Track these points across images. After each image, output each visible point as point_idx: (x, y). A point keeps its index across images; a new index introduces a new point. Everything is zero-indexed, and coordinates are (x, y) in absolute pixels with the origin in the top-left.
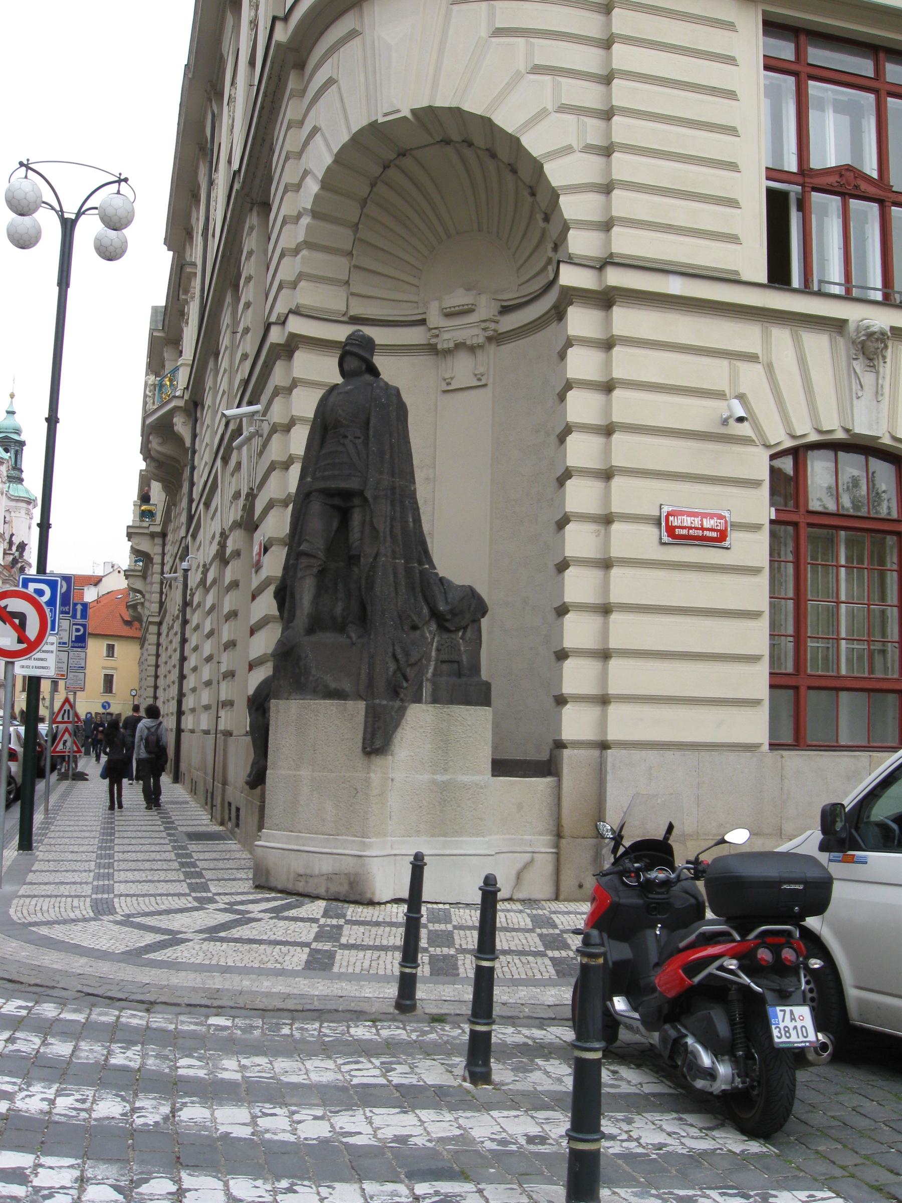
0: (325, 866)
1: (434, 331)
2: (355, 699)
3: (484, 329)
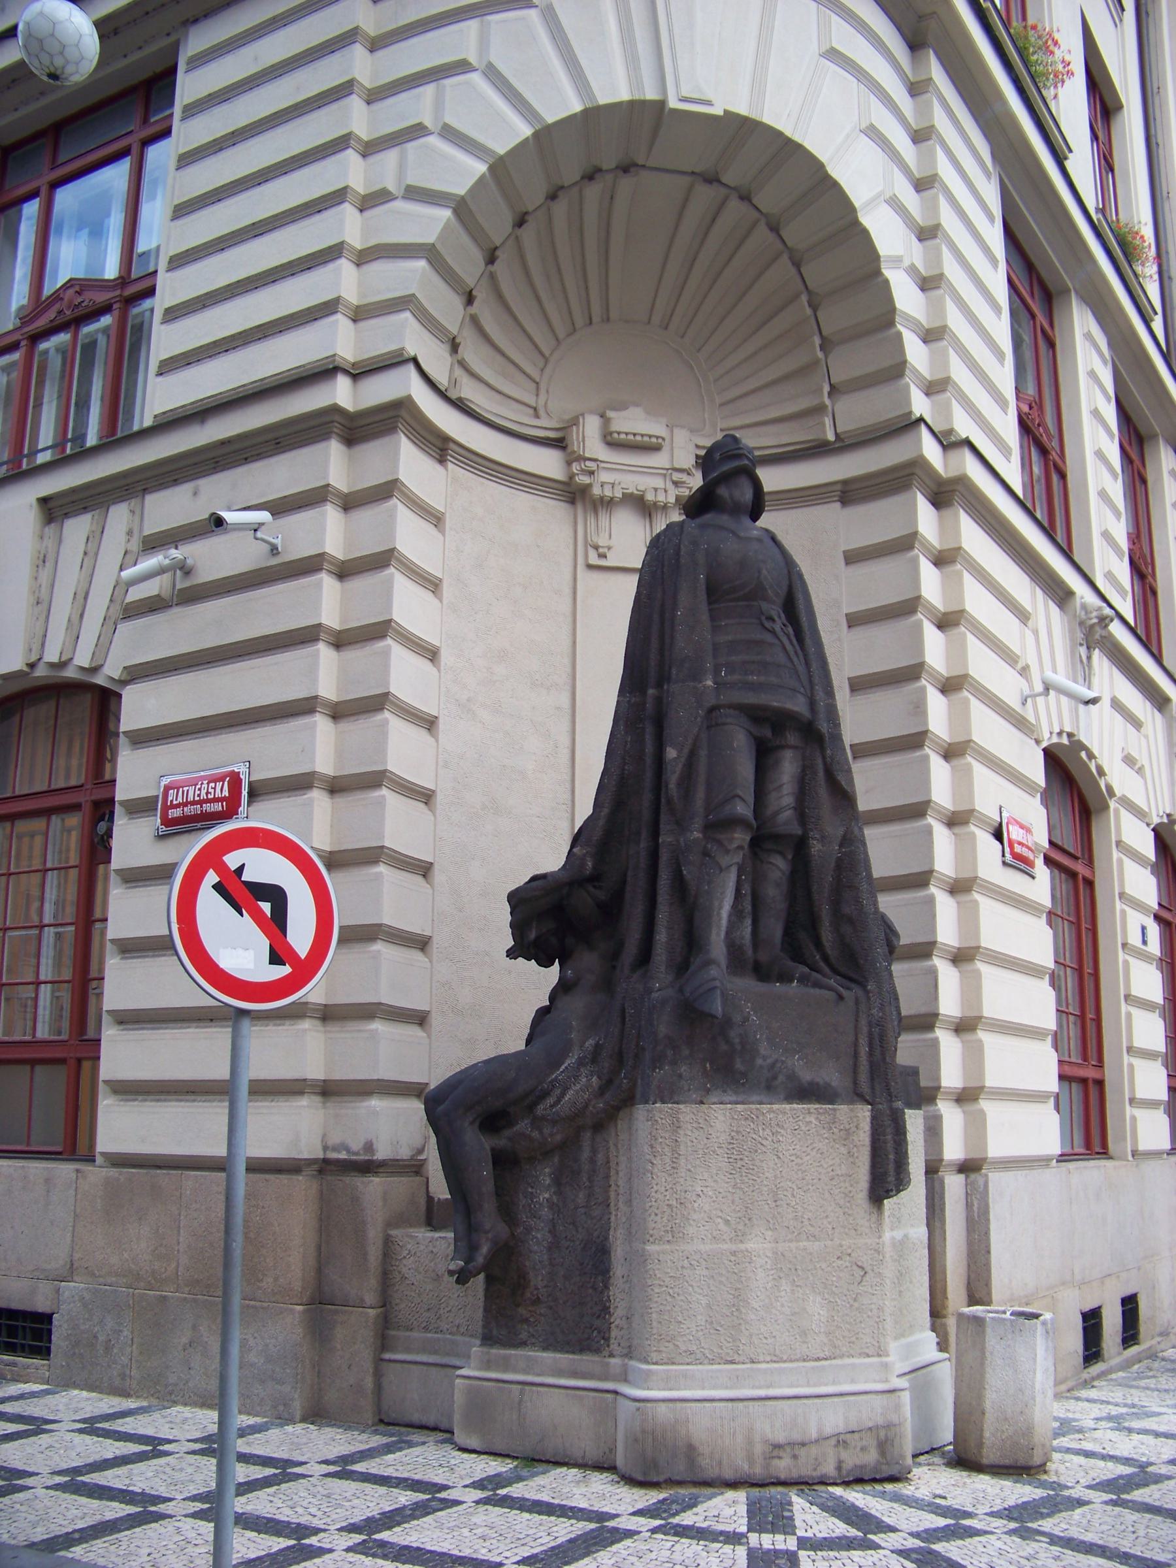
0: (832, 1419)
1: (588, 463)
2: (851, 1102)
3: (676, 484)
